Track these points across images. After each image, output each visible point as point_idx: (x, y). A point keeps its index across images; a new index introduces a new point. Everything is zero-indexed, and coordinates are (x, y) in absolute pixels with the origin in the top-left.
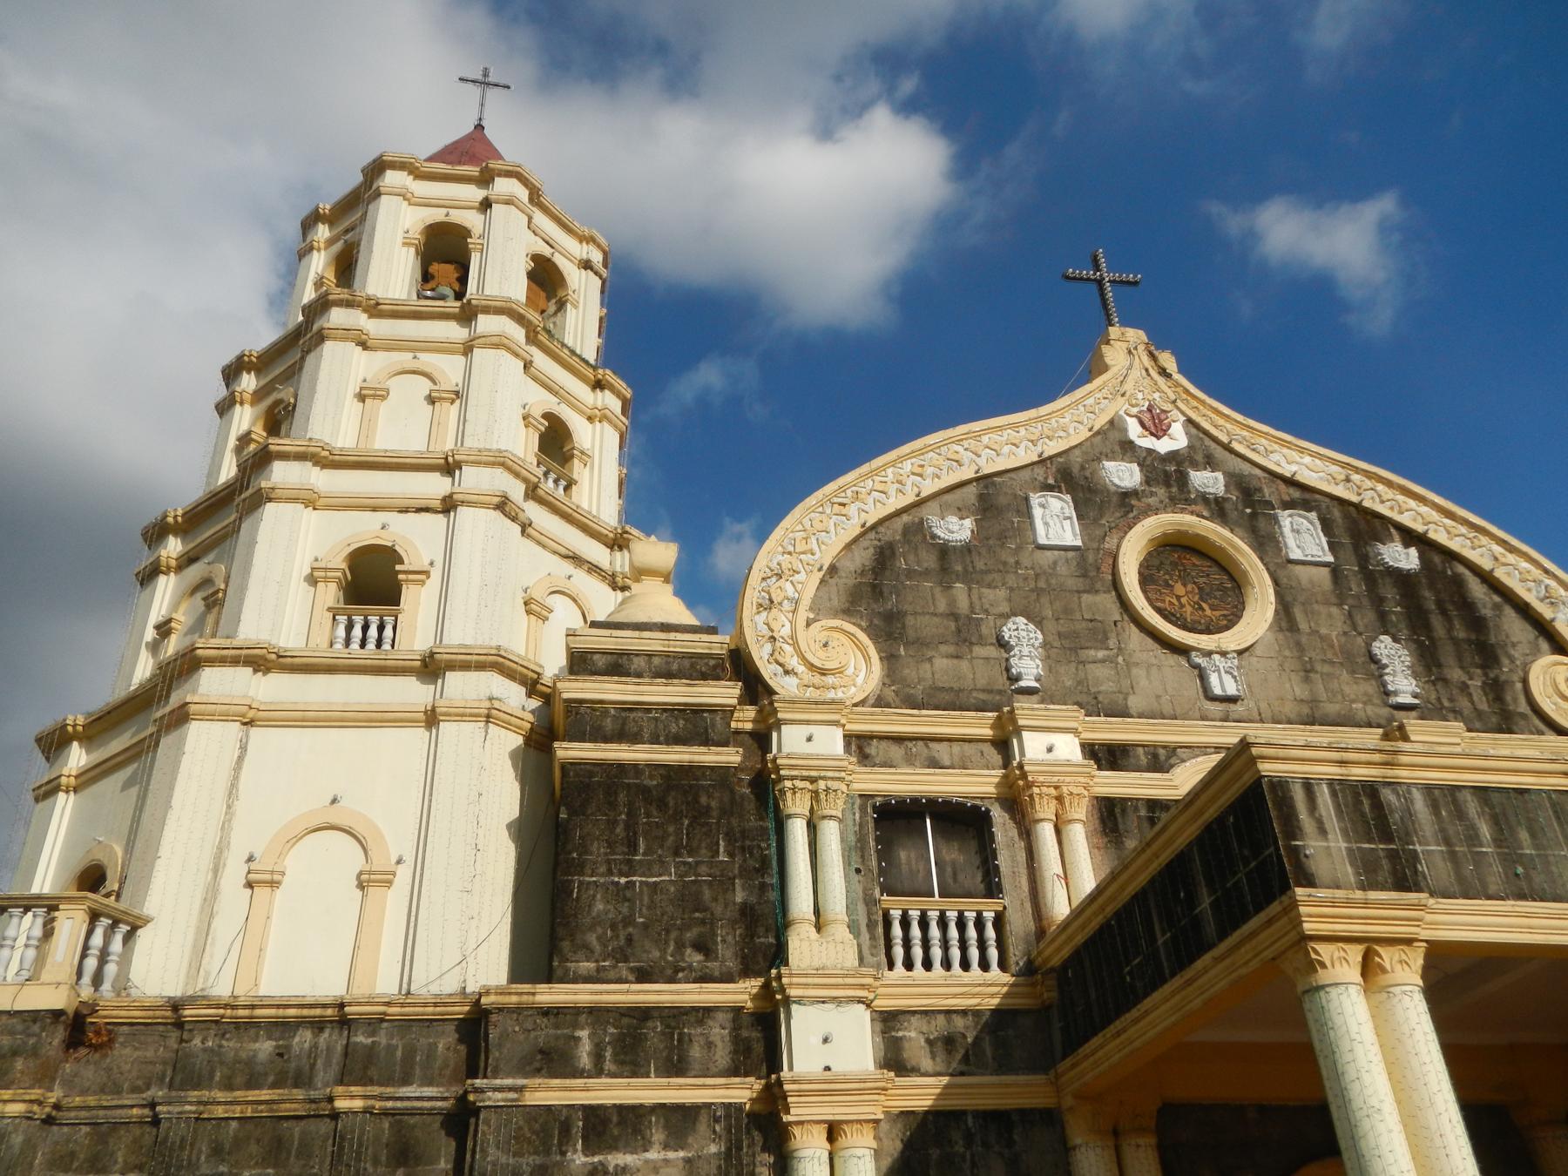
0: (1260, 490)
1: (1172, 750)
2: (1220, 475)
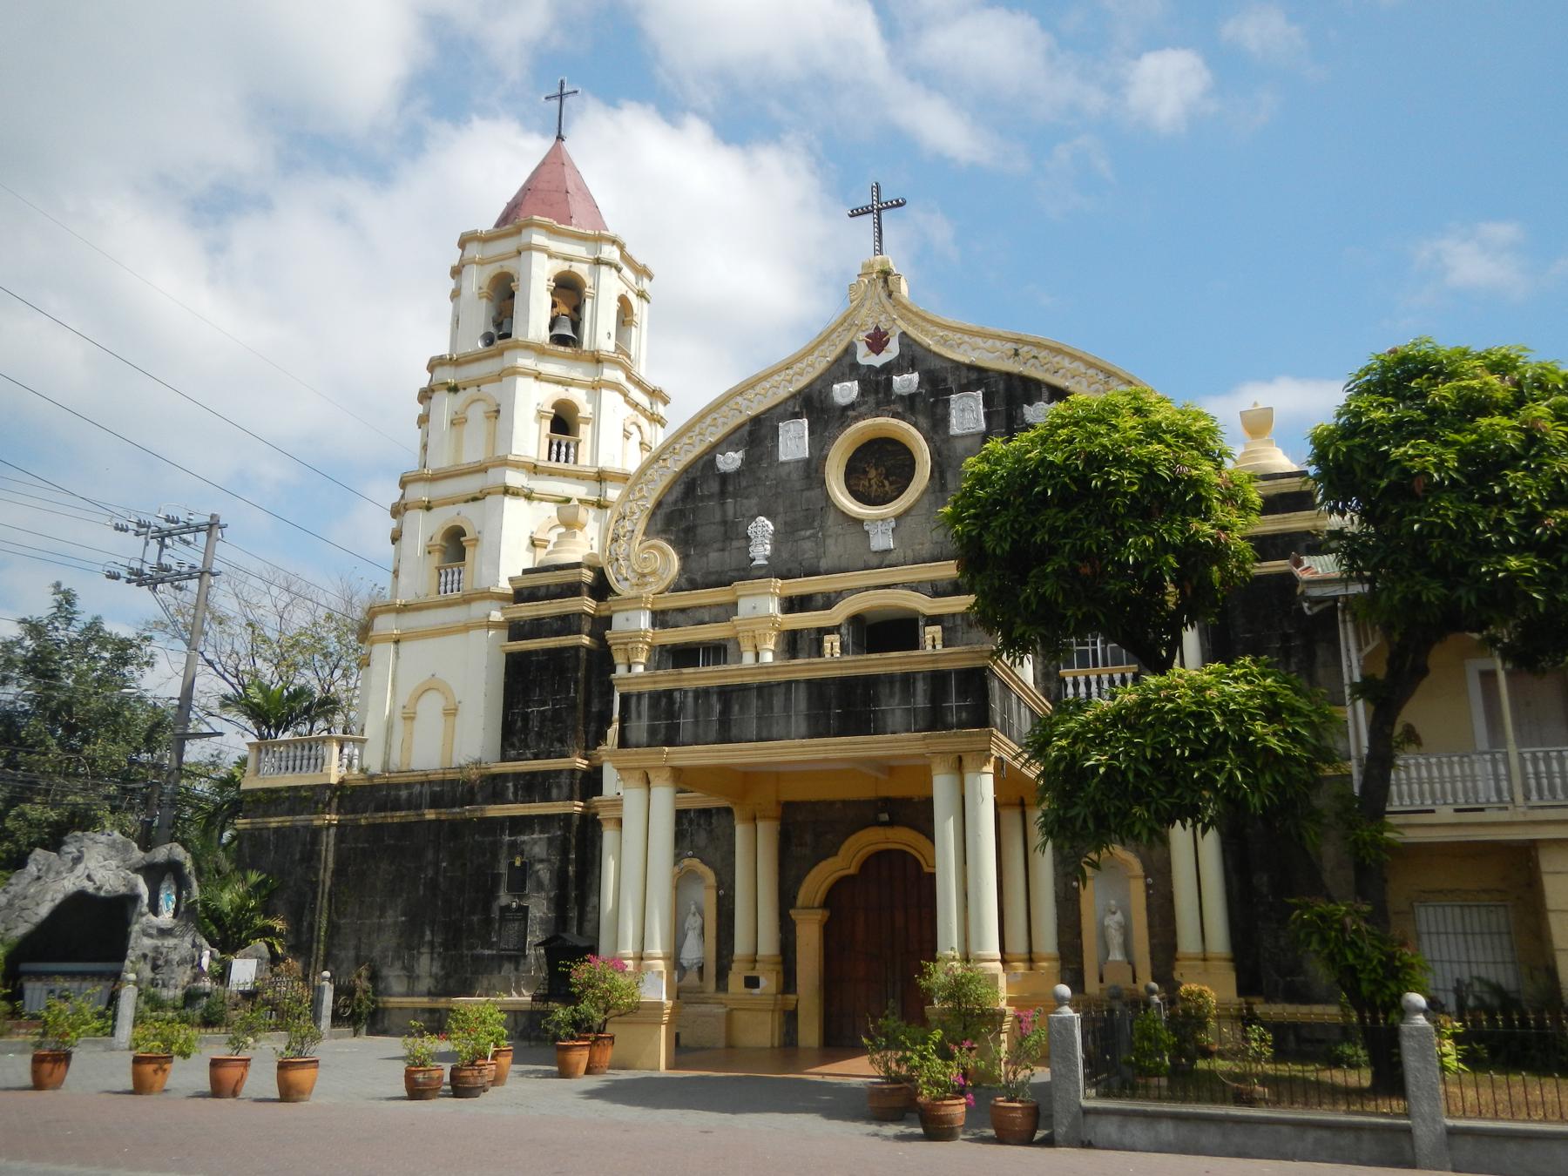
0: (945, 380)
1: (840, 595)
2: (915, 377)
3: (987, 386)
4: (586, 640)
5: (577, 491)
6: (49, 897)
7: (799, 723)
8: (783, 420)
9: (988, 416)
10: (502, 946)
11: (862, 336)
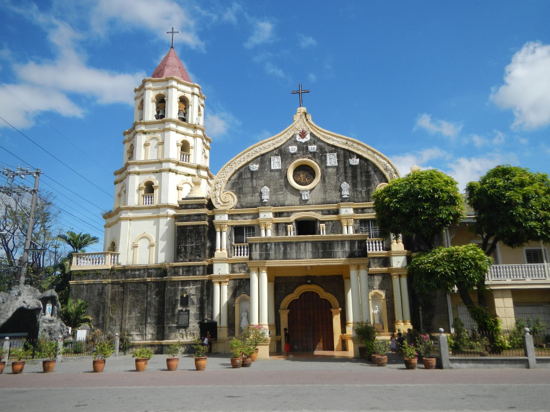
0: (325, 149)
1: (292, 212)
2: (315, 147)
3: (338, 152)
4: (207, 223)
5: (193, 171)
6: (11, 309)
7: (309, 254)
8: (271, 155)
9: (338, 161)
10: (180, 323)
11: (298, 132)
